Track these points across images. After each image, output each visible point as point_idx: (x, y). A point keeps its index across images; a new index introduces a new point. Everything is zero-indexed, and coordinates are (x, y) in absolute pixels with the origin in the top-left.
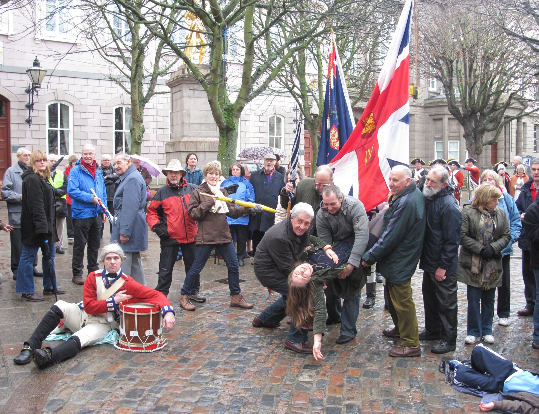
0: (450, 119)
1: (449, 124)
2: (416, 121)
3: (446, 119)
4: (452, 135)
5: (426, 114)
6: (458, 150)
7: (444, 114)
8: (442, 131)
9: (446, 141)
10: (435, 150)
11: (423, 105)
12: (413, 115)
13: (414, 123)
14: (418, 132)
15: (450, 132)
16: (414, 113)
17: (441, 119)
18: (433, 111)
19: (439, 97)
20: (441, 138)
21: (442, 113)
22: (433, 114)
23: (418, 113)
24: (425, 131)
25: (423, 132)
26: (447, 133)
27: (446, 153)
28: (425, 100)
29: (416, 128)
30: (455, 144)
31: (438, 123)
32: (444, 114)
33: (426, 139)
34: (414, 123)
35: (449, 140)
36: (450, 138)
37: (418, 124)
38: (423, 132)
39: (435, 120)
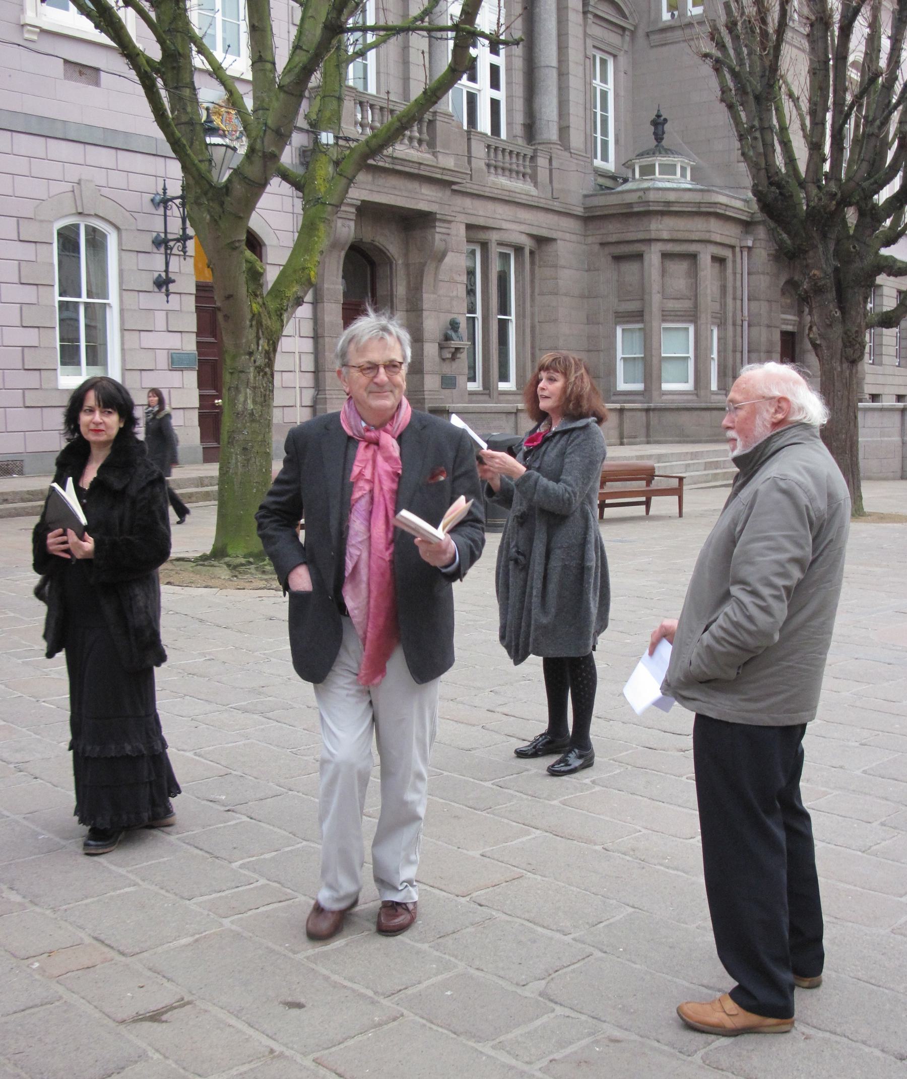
0: (665, 256)
1: (664, 272)
2: (562, 262)
3: (653, 257)
4: (671, 305)
5: (590, 240)
6: (691, 354)
7: (649, 241)
8: (642, 293)
9: (655, 324)
10: (619, 354)
11: (579, 211)
12: (553, 240)
13: (555, 266)
14: (566, 295)
15: (664, 297)
16: (553, 235)
17: (639, 257)
18: (614, 231)
19: (629, 186)
20: (638, 316)
21: (641, 236)
22: (613, 238)
23: (567, 236)
24: (588, 295)
25: (582, 296)
26: (656, 299)
27: (655, 361)
28: (585, 196)
29: (561, 283)
30: (681, 335)
31: (630, 269)
32: (649, 241)
33: (591, 320)
34: (555, 266)
35: (664, 321)
36: (666, 316)
37: (566, 271)
38: (582, 296)
39: (618, 258)
